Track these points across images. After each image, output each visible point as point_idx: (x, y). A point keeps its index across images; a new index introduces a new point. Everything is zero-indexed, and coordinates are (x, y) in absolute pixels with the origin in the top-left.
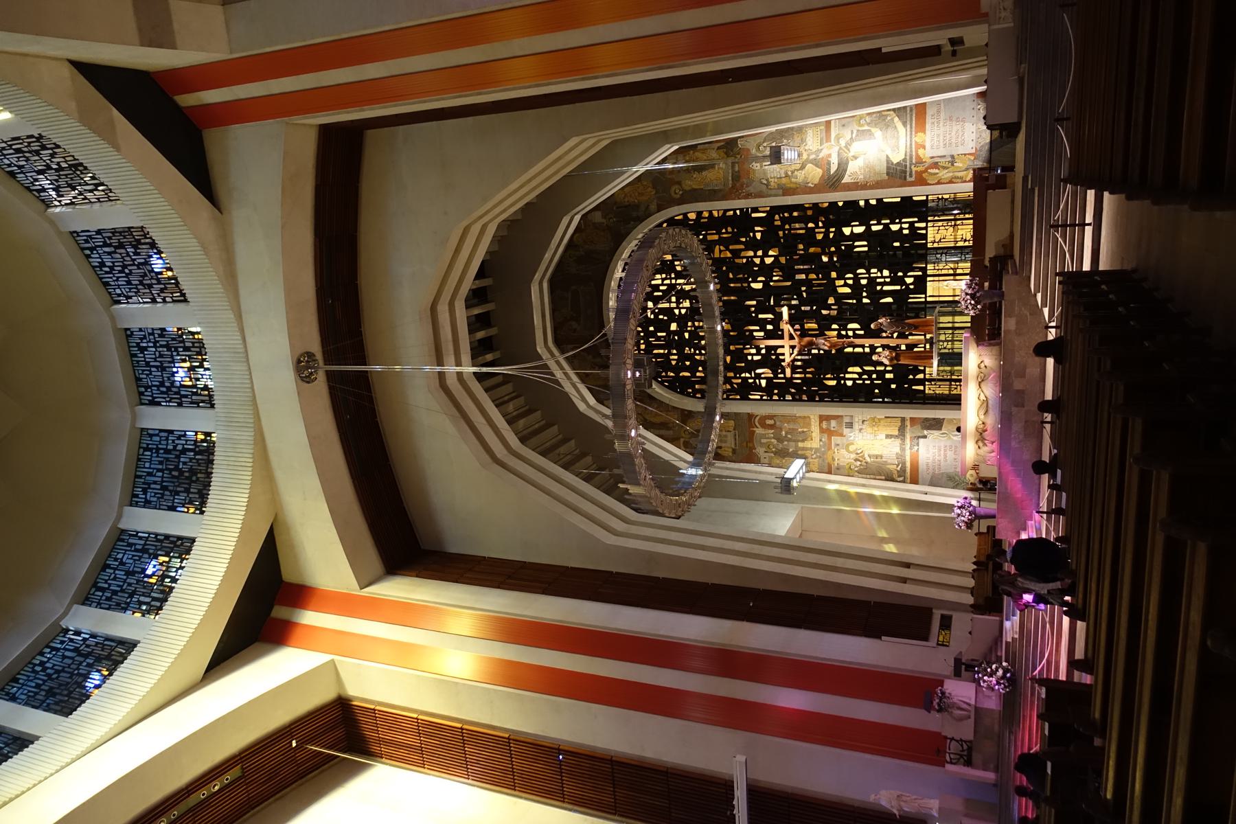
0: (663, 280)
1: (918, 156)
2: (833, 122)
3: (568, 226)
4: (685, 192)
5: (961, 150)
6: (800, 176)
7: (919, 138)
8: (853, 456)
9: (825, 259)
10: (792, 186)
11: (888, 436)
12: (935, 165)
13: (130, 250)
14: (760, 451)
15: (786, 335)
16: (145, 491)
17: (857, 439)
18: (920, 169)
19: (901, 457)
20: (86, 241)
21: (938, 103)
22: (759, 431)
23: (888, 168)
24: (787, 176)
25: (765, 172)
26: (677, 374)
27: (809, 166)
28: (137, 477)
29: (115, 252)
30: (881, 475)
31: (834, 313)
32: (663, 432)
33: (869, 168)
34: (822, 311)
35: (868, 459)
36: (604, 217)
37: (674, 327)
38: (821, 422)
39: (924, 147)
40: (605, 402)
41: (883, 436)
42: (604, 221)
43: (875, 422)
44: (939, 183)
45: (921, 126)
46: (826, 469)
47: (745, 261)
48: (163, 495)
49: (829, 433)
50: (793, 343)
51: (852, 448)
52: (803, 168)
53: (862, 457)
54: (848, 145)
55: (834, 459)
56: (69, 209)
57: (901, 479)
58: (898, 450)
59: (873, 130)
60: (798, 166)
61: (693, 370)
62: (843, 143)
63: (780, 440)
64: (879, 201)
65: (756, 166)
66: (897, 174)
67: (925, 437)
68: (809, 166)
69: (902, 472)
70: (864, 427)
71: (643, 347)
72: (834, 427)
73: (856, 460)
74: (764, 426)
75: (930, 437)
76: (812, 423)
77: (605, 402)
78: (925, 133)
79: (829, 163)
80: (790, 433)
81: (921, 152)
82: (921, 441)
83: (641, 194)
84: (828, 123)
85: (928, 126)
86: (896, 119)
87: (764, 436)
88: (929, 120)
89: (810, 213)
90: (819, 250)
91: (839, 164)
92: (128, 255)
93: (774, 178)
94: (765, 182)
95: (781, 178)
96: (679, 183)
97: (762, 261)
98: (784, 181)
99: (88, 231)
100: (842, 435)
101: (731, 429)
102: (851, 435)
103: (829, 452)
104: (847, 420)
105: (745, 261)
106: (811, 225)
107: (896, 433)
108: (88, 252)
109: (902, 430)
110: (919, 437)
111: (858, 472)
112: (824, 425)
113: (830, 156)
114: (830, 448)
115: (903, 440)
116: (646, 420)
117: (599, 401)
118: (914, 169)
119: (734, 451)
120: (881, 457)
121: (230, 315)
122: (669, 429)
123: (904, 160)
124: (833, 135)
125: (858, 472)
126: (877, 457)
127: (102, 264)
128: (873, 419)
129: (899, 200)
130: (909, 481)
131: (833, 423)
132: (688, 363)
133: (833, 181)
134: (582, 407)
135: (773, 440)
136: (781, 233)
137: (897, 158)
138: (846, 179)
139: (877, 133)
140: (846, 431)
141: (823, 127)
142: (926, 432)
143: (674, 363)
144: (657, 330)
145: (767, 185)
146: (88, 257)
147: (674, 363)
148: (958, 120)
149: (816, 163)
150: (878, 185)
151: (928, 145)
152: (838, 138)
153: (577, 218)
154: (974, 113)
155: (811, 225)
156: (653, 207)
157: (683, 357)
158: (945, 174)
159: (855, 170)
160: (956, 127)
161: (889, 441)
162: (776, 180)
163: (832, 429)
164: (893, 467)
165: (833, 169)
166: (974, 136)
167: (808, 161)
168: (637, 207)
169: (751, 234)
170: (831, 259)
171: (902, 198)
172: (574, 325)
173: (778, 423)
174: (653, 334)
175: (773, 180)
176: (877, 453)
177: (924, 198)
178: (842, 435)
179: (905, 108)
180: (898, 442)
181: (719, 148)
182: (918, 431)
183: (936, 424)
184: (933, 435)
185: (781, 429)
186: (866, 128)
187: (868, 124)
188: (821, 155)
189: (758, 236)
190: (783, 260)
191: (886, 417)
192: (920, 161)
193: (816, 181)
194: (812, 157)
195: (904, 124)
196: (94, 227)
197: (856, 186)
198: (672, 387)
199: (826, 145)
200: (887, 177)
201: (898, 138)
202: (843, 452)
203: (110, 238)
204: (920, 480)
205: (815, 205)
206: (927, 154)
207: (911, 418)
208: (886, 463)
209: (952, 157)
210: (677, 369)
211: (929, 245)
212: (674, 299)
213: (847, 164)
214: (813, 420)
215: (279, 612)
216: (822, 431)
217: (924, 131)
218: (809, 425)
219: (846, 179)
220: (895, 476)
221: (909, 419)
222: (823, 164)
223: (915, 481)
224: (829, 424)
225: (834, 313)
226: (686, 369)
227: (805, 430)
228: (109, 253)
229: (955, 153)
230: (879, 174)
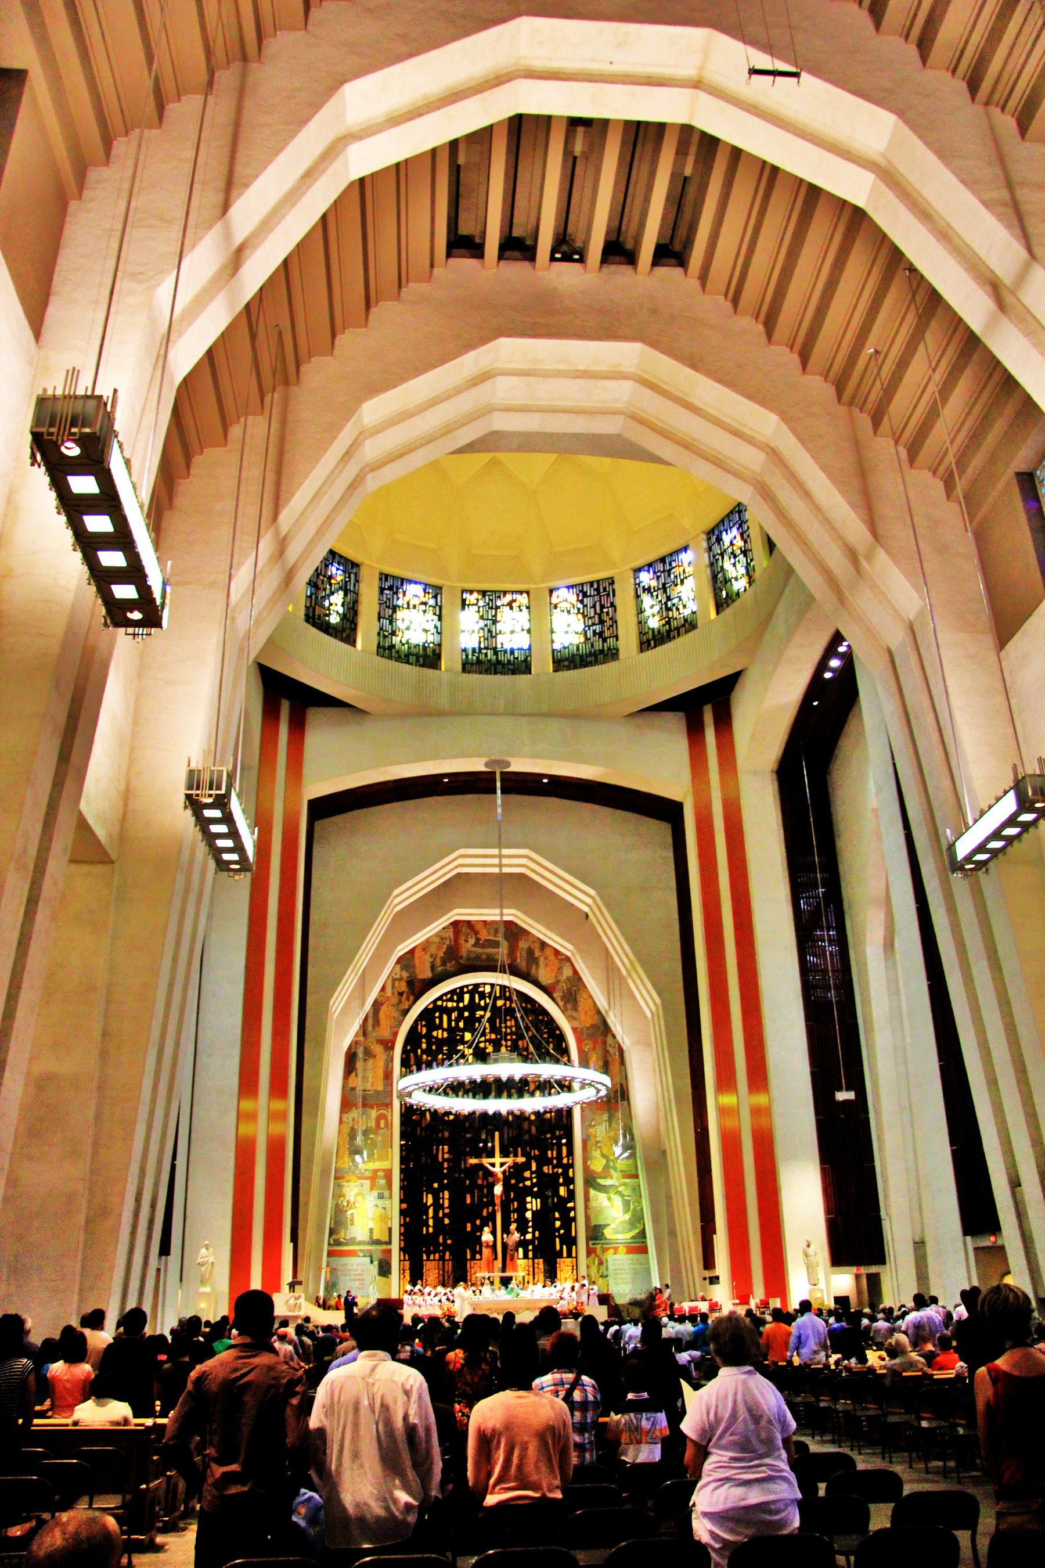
0: (511, 1027)
1: (608, 1249)
2: (636, 1180)
3: (566, 947)
4: (587, 1054)
5: (611, 1282)
6: (597, 1154)
7: (622, 1249)
8: (352, 1200)
9: (527, 1174)
10: (589, 1147)
11: (371, 1231)
12: (601, 1263)
13: (598, 628)
14: (354, 1113)
15: (504, 1160)
16: (391, 588)
18: (599, 1251)
19: (353, 1241)
20: (605, 589)
21: (647, 1263)
22: (374, 1113)
23: (600, 1226)
24: (598, 1142)
25: (600, 1124)
26: (425, 1036)
27: (604, 1161)
28: (402, 580)
29: (595, 613)
30: (336, 1223)
31: (480, 1182)
32: (370, 1021)
33: (600, 1211)
35: (349, 1213)
36: (568, 979)
37: (468, 1036)
38: (383, 1170)
39: (615, 1253)
40: (398, 966)
41: (371, 1225)
42: (565, 977)
43: (384, 1218)
44: (588, 1266)
45: (631, 1250)
46: (339, 1175)
48: (388, 607)
49: (373, 1177)
50: (498, 1165)
51: (359, 1198)
52: (603, 1156)
53: (351, 1208)
54: (619, 1193)
55: (348, 1181)
56: (632, 593)
57: (332, 1242)
58: (359, 1238)
59: (630, 1213)
60: (605, 1152)
61: (428, 1051)
62: (620, 1189)
63: (365, 1133)
64: (574, 1219)
65: (605, 1116)
66: (595, 1233)
67: (372, 1262)
68: (604, 1161)
69: (338, 1243)
70: (380, 1209)
71: (450, 1004)
73: (348, 1202)
74: (379, 1118)
75: (371, 1267)
77: (398, 966)
78: (627, 1253)
79: (605, 1177)
80: (372, 1143)
81: (612, 1251)
82: (368, 1259)
83: (586, 1013)
84: (636, 1176)
85: (631, 1256)
86: (637, 1231)
87: (369, 1117)
88: (635, 1256)
89: (565, 1161)
90: (534, 1168)
91: (604, 1186)
92: (593, 624)
96: (594, 1049)
98: (593, 1140)
99: (614, 595)
100: (372, 1188)
101: (375, 1087)
103: (355, 1179)
104: (386, 1193)
106: (555, 1162)
107: (375, 1237)
108: (595, 586)
109: (378, 1242)
110: (371, 1257)
111: (337, 1205)
112: (381, 1174)
113: (611, 1178)
114: (359, 1178)
115: (368, 1243)
116: (382, 1004)
117: (399, 961)
118: (598, 1247)
119: (353, 1089)
120: (352, 1224)
121: (545, 708)
122: (374, 1027)
123: (606, 1239)
124: (627, 1181)
125: (337, 1205)
126: (352, 1220)
127: (585, 595)
128: (386, 1217)
129: (573, 1234)
130: (331, 1248)
131: (383, 1182)
132: (434, 1047)
133: (591, 1181)
134: (399, 948)
136: (548, 1136)
137: (608, 1233)
138: (592, 1192)
139: (627, 1217)
140: (375, 1193)
141: (633, 1172)
142: (376, 1263)
143: (435, 1033)
144: (466, 1020)
145: (590, 1126)
146: (592, 584)
147: (435, 1033)
148: (634, 1278)
149: (606, 1167)
150: (587, 1218)
151: (615, 1256)
152: (625, 1184)
153: (569, 954)
154: (639, 1291)
155: (555, 1162)
156: (576, 1024)
157: (441, 1043)
158: (594, 1270)
159: (599, 1199)
160: (629, 1278)
161: (368, 1231)
164: (342, 1234)
165: (601, 1181)
166: (621, 1291)
167: (608, 1160)
168: (575, 1008)
170: (527, 1179)
171: (576, 1237)
172: (472, 941)
173: (381, 1131)
174: (460, 1017)
176: (356, 1220)
177: (574, 1255)
179: (645, 1237)
180: (366, 1238)
181: (621, 1085)
182: (377, 1257)
183: (384, 1270)
184: (374, 1269)
185: (376, 1134)
186: (632, 1207)
187: (634, 1209)
188: (612, 1171)
190: (526, 1137)
191: (390, 1229)
192: (605, 1250)
193: (592, 1167)
194: (611, 1164)
195: (633, 1237)
196: (618, 601)
197: (587, 1199)
198: (413, 1029)
199: (620, 1175)
200: (593, 1223)
201: (622, 1232)
202: (356, 1190)
203: (608, 613)
204: (331, 1259)
205: (571, 1166)
206: (610, 1257)
207: (390, 1251)
208: (346, 1228)
209: (607, 1276)
210: (429, 1036)
211: (536, 1261)
212: (493, 1036)
213: (606, 1192)
215: (285, 707)
216: (376, 1171)
217: (627, 1253)
218: (380, 1159)
219: (592, 1192)
220: (334, 1237)
221: (389, 1247)
222: (606, 1173)
223: (330, 1254)
224: (381, 1178)
225: (480, 1182)
226: (429, 1044)
228: (594, 606)
229: (609, 1278)
230: (596, 1219)
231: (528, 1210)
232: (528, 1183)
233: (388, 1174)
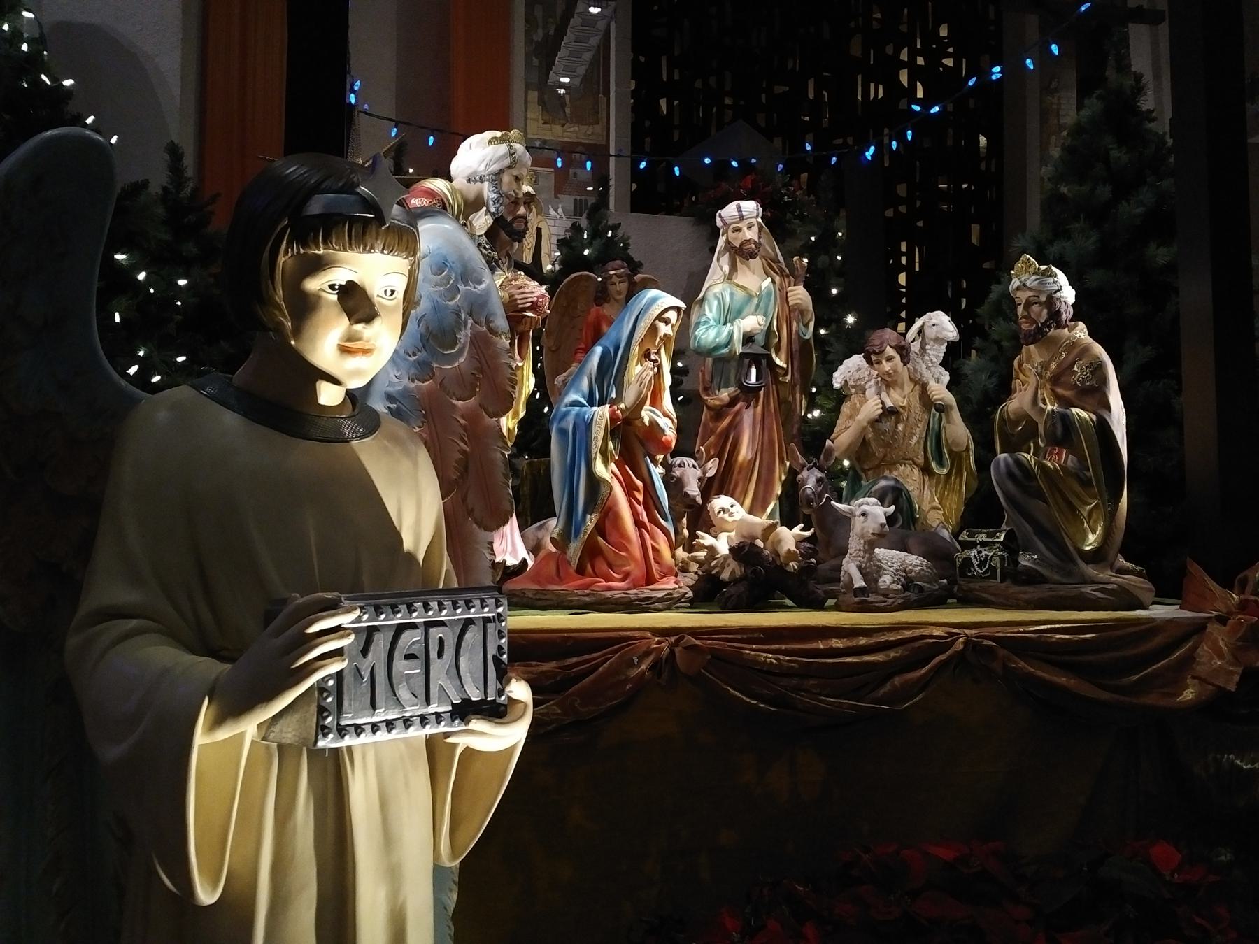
17: (551, 222)
34: (806, 174)
47: (904, 28)
72: (575, 175)
76: (584, 128)
93: (1059, 104)
94: (1052, 86)
95: (1058, 116)
97: (903, 65)
100: (558, 190)
102: (560, 210)
105: (904, 28)
135: (540, 32)
140: (568, 200)
162: (1055, 107)
163: (571, 171)
169: (951, 50)
175: (1055, 100)
178: (558, 190)
189: (949, 62)
214: (590, 131)
218: (579, 120)
227: (568, 111)
231: (901, 268)
232: (903, 209)
233: (598, 153)
